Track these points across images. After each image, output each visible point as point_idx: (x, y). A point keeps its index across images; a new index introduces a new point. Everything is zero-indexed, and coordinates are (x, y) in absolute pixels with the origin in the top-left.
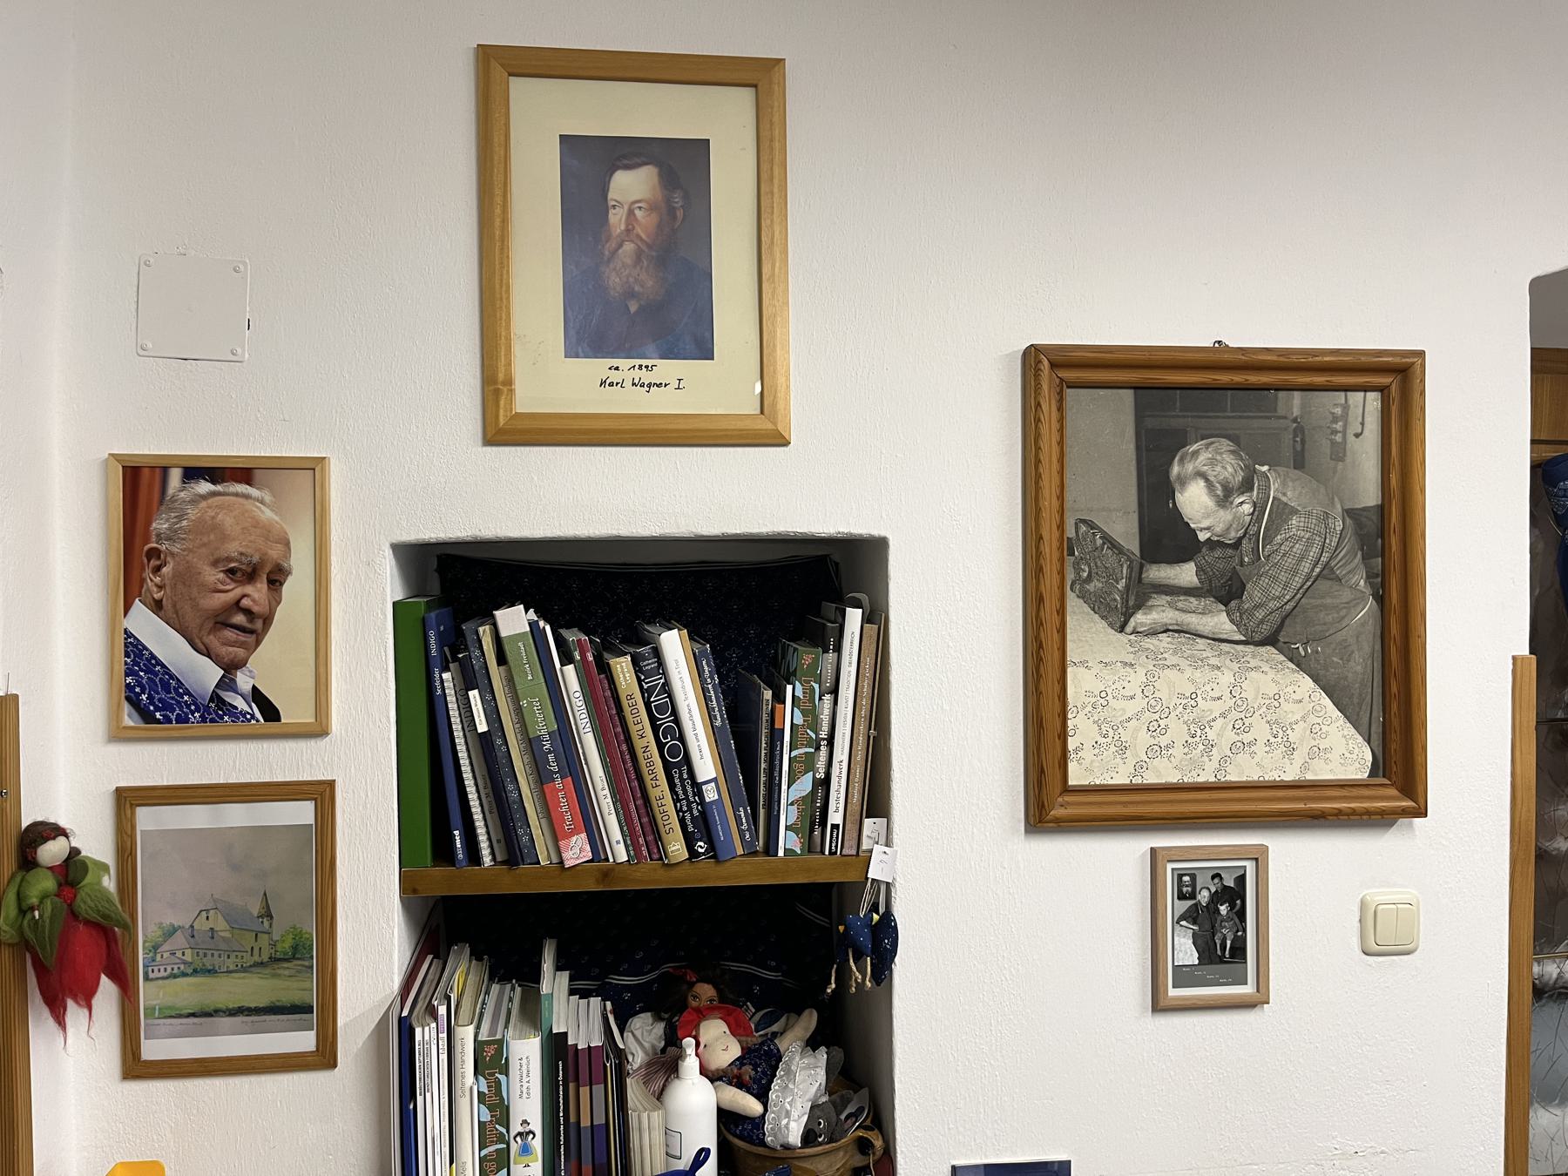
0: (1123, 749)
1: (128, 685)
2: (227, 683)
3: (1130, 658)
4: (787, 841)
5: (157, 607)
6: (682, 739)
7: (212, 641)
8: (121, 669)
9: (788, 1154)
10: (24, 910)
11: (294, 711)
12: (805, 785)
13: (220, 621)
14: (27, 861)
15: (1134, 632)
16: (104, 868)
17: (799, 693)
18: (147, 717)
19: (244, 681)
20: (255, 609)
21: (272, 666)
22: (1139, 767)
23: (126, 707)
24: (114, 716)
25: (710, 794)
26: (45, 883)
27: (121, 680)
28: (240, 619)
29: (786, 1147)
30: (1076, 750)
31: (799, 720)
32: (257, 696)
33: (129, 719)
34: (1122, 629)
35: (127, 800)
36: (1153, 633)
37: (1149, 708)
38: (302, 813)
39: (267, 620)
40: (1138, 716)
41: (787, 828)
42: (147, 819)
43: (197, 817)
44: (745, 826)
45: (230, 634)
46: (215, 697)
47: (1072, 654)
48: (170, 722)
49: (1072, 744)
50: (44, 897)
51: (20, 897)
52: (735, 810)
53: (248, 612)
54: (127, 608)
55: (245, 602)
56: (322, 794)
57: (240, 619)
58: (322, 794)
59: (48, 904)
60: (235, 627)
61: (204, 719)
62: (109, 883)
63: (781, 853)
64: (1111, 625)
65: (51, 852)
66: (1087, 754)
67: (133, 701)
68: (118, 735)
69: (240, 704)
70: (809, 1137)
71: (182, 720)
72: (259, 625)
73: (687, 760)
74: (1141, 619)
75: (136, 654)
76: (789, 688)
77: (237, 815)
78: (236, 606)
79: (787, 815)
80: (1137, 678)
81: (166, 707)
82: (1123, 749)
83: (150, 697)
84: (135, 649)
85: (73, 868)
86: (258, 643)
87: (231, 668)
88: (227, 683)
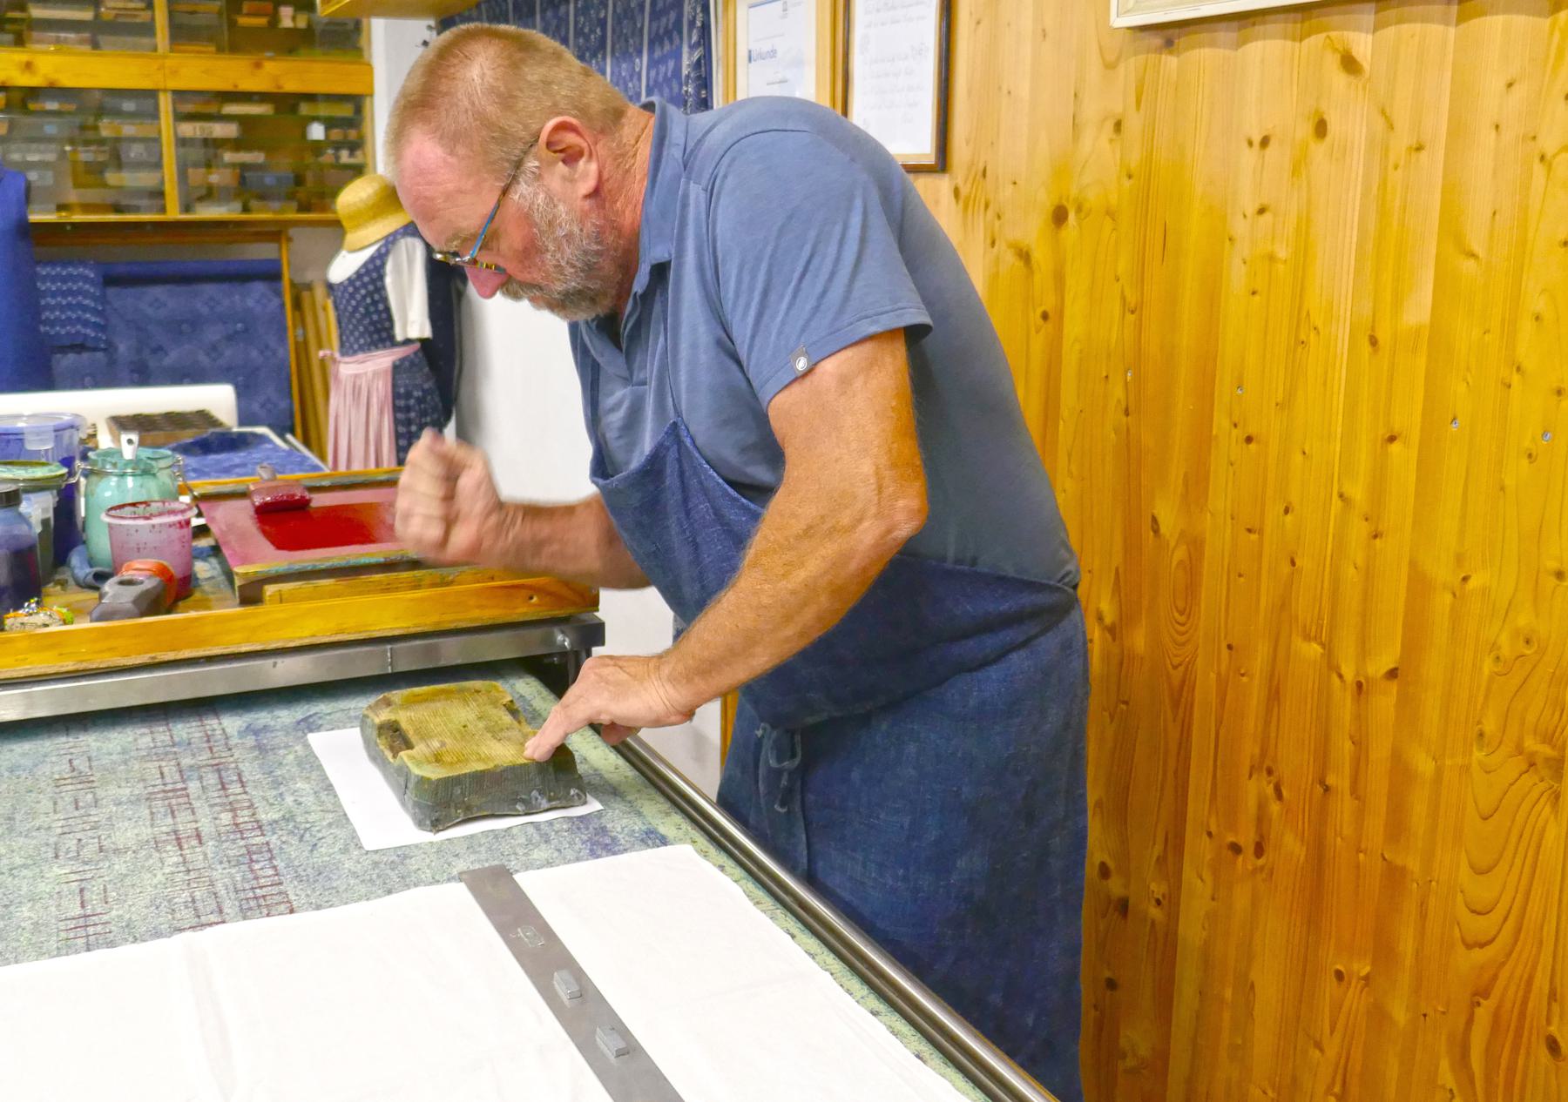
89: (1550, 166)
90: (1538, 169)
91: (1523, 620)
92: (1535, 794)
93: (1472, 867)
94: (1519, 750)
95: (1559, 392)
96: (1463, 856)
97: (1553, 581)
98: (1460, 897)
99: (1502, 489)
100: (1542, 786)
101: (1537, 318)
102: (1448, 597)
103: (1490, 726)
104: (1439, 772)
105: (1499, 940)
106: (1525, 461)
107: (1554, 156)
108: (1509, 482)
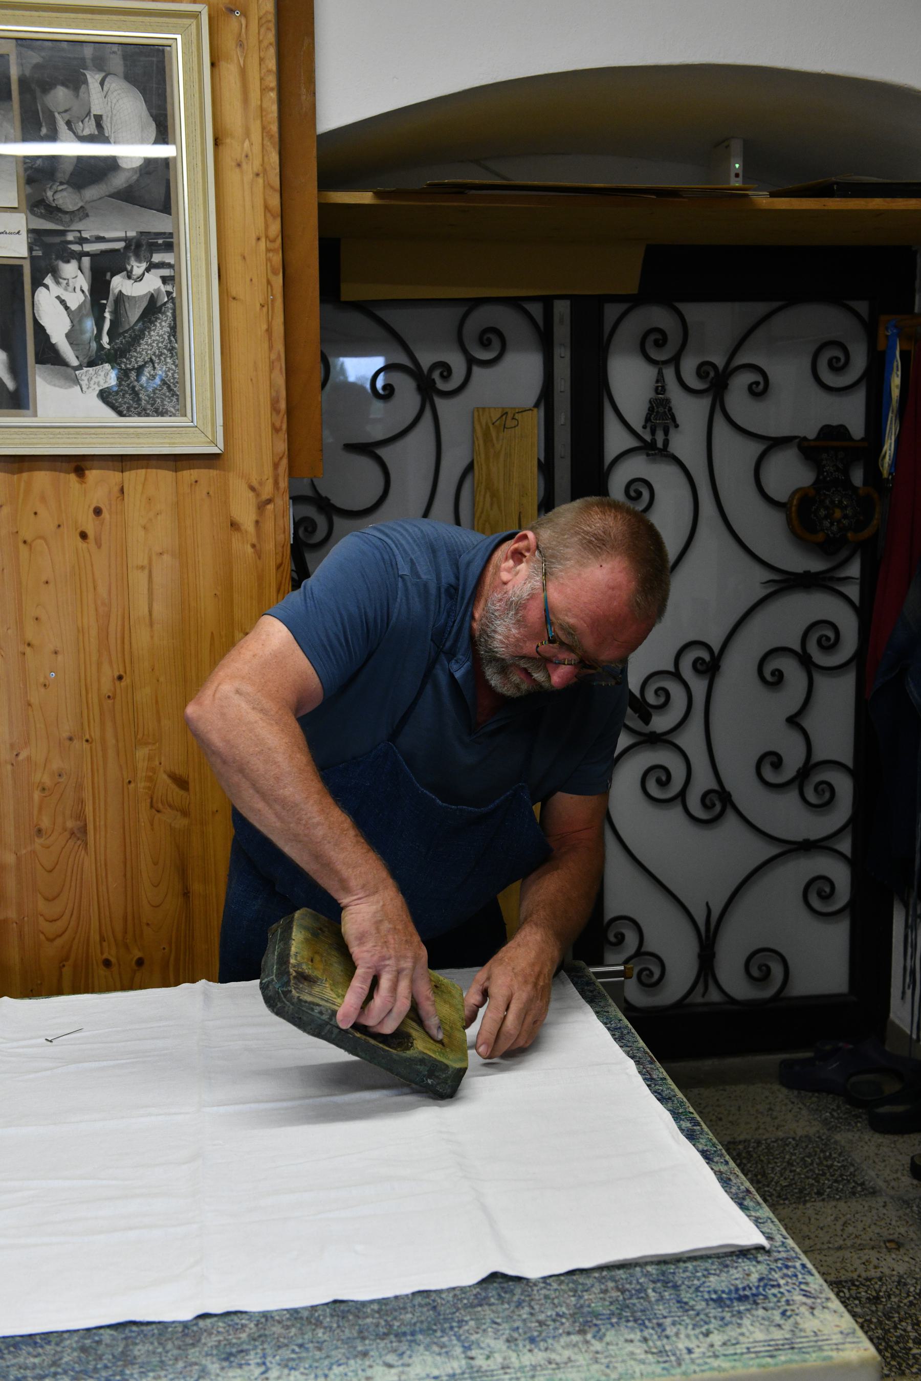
89: (31, 545)
90: (23, 549)
91: (56, 764)
92: (76, 847)
93: (47, 899)
94: (65, 829)
95: (56, 653)
96: (39, 896)
97: (67, 743)
98: (41, 919)
99: (30, 705)
100: (79, 842)
101: (37, 619)
102: (9, 767)
103: (45, 823)
104: (19, 859)
105: (67, 934)
106: (42, 690)
107: (33, 541)
108: (34, 700)
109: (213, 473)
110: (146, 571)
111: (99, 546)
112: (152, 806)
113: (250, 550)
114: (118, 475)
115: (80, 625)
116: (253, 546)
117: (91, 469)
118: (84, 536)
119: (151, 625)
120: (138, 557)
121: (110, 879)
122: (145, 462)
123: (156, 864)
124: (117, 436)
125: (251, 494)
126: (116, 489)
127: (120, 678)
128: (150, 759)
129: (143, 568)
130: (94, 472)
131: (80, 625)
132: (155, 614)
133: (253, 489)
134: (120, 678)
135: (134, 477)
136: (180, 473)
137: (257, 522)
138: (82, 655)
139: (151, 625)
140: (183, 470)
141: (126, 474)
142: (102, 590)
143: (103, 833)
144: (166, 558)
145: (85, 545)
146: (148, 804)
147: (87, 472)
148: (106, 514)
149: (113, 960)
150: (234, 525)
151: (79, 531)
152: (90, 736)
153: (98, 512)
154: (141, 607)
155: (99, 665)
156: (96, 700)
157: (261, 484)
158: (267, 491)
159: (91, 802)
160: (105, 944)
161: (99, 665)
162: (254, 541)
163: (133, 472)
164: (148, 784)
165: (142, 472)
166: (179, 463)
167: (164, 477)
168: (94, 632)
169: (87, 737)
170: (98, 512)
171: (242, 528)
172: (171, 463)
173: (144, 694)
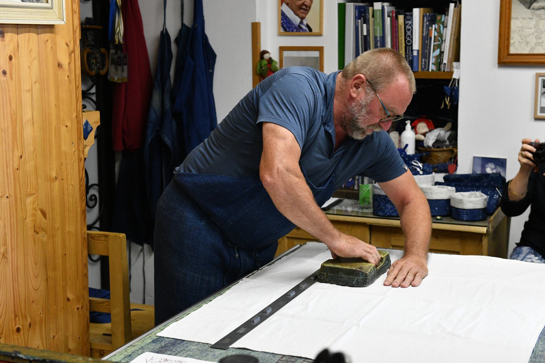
0: (527, 43)
1: (282, 23)
2: (301, 22)
3: (531, 17)
4: (432, 67)
5: (287, 4)
6: (412, 39)
7: (298, 12)
8: (280, 19)
9: (429, 150)
10: (261, 67)
11: (315, 30)
12: (437, 52)
13: (300, 7)
14: (262, 58)
15: (533, 9)
16: (276, 63)
17: (436, 27)
18: (285, 30)
19: (305, 22)
20: (308, 5)
21: (310, 19)
22: (532, 49)
23: (281, 28)
24: (279, 29)
25: (415, 53)
26: (265, 62)
27: (281, 21)
28: (304, 7)
29: (429, 147)
30: (513, 44)
31: (436, 34)
32: (308, 26)
33: (282, 30)
34: (529, 8)
35: (282, 49)
36: (539, 9)
37: (536, 31)
38: (316, 54)
39: (310, 7)
40: (532, 34)
41: (432, 64)
42: (286, 54)
43: (295, 54)
44: (423, 64)
45: (302, 11)
46: (299, 26)
47: (513, 15)
48: (289, 31)
49: (512, 41)
50: (265, 65)
51: (261, 65)
52: (422, 59)
53: (306, 6)
54: (282, 4)
55: (305, 3)
56: (320, 49)
57: (304, 7)
58: (320, 49)
59: (266, 67)
60: (303, 9)
61: (297, 31)
62: (278, 66)
63: (430, 70)
64: (526, 7)
65: (266, 56)
66: (517, 45)
67: (283, 26)
68: (280, 35)
69: (304, 27)
70: (433, 145)
71: (292, 31)
72: (308, 8)
73: (412, 45)
74: (535, 5)
75: (283, 16)
76: (434, 26)
77: (304, 54)
78: (303, 4)
79: (432, 60)
80: (533, 22)
81: (289, 28)
82: (527, 43)
83: (287, 26)
84: (283, 14)
85: (270, 60)
86: (308, 13)
87: (302, 18)
88: (301, 22)
109: (53, 35)
110: (30, 93)
111: (12, 79)
112: (35, 231)
113: (67, 78)
114: (15, 35)
115: (3, 127)
116: (68, 77)
117: (7, 33)
118: (4, 73)
119: (33, 124)
120: (26, 86)
121: (19, 278)
122: (27, 29)
123: (36, 264)
124: (23, 13)
125: (67, 47)
126: (16, 45)
127: (21, 157)
128: (34, 203)
129: (29, 91)
130: (9, 34)
131: (3, 127)
132: (34, 118)
133: (67, 45)
134: (21, 157)
135: (24, 37)
136: (40, 36)
137: (69, 63)
138: (4, 145)
139: (33, 124)
140: (41, 34)
141: (20, 36)
142: (14, 106)
143: (16, 252)
144: (37, 84)
145: (5, 79)
146: (33, 230)
147: (5, 34)
148: (13, 60)
149: (21, 327)
150: (60, 65)
151: (2, 70)
152: (9, 194)
153: (11, 58)
154: (27, 115)
155: (13, 151)
156: (12, 173)
157: (70, 42)
158: (71, 45)
159: (10, 234)
160: (17, 319)
161: (13, 151)
162: (68, 74)
163: (23, 35)
164: (33, 218)
165: (27, 34)
166: (39, 30)
167: (33, 36)
168: (10, 131)
169: (7, 195)
170: (11, 58)
171: (64, 66)
172: (34, 29)
173: (30, 166)
